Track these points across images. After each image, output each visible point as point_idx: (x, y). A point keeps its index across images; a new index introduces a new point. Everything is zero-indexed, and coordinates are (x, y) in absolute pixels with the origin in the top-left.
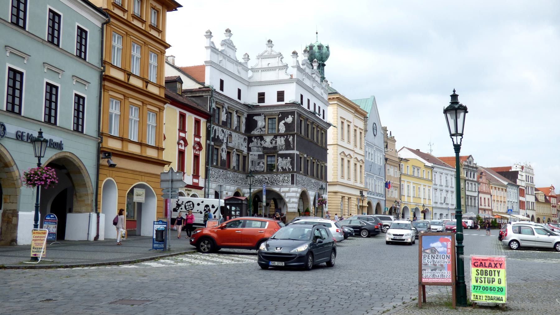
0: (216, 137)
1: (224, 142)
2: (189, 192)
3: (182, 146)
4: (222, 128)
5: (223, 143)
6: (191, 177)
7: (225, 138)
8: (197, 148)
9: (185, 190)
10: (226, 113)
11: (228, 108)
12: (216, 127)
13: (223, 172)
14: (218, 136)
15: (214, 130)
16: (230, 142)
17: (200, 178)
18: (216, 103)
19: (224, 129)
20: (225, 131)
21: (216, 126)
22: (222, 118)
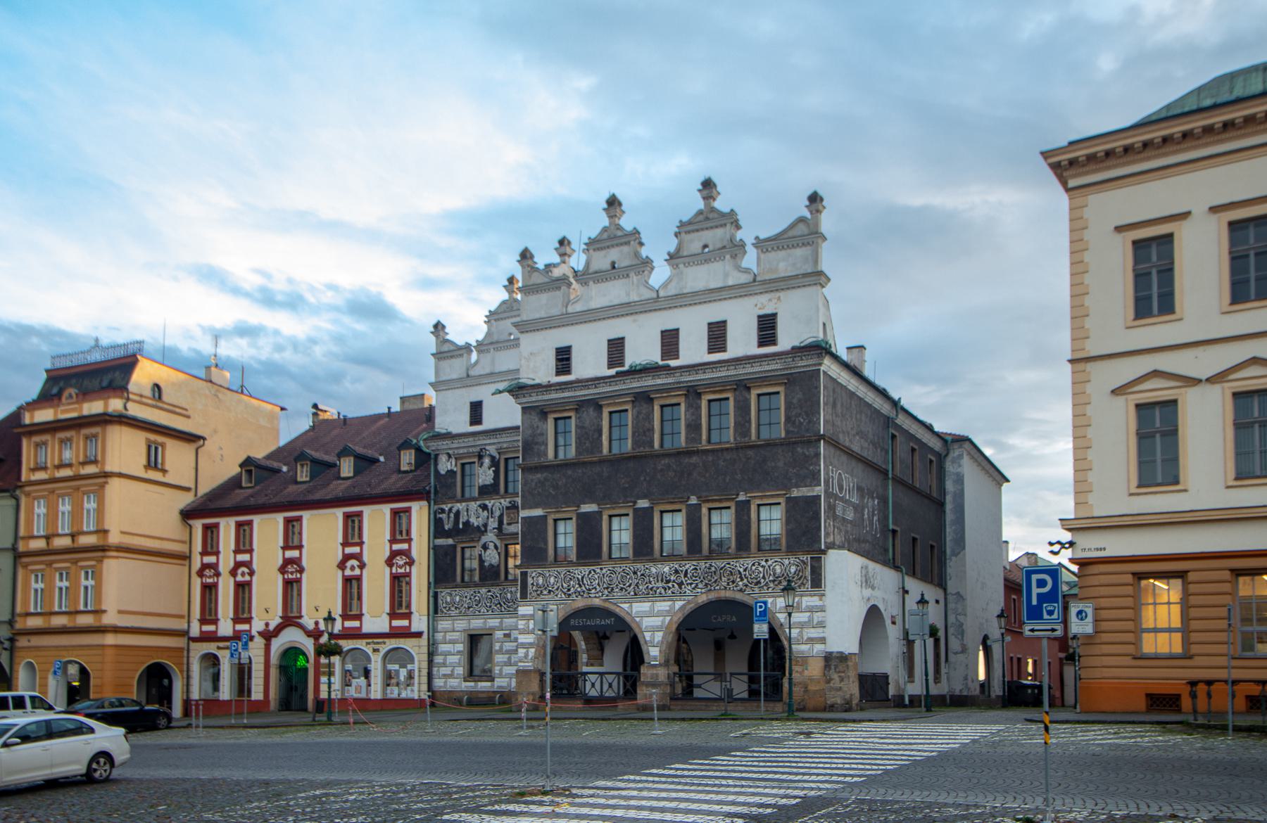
0: (461, 526)
1: (489, 528)
2: (376, 647)
3: (353, 568)
4: (478, 503)
5: (486, 531)
6: (386, 618)
7: (491, 520)
8: (401, 563)
9: (364, 644)
10: (495, 463)
11: (499, 453)
12: (458, 506)
13: (489, 591)
14: (467, 524)
15: (452, 515)
16: (509, 524)
17: (415, 617)
18: (456, 458)
19: (487, 502)
20: (490, 505)
21: (458, 505)
22: (480, 481)
